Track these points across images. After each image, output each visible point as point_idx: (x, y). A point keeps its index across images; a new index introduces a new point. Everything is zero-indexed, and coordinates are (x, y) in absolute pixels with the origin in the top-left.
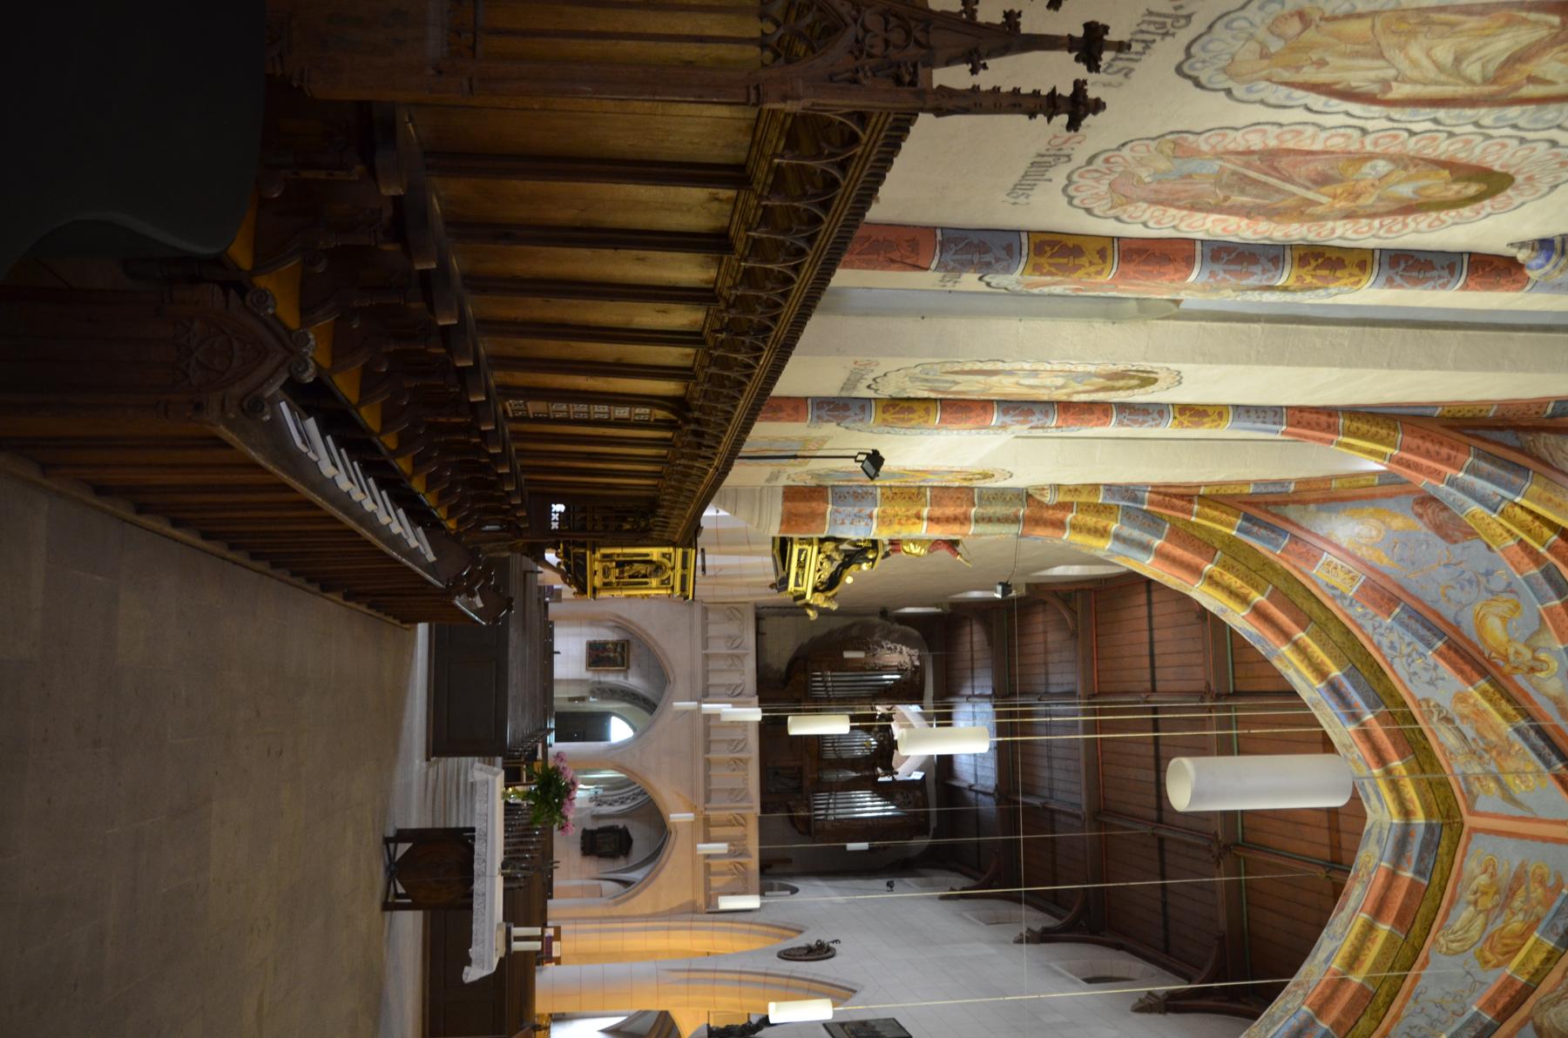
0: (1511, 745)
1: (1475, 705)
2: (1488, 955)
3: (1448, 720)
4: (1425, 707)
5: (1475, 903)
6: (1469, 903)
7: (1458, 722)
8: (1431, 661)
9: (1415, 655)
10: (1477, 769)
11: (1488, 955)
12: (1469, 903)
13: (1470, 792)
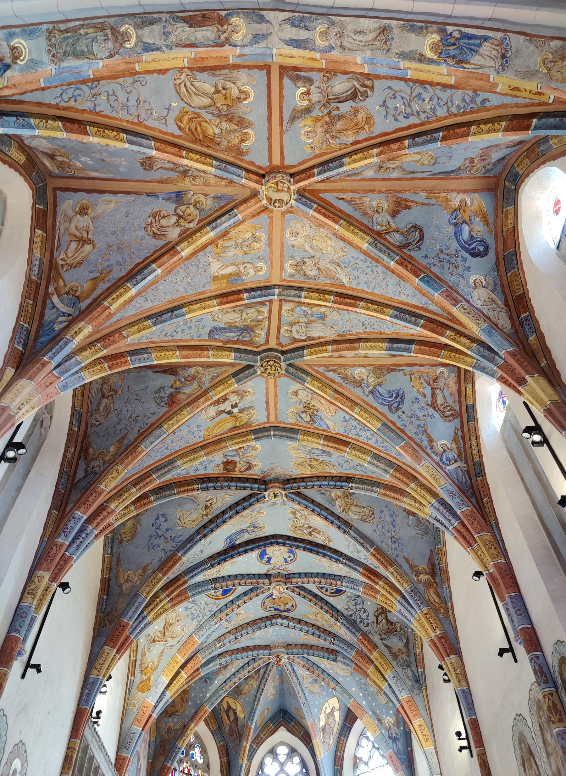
0: (333, 137)
1: (362, 128)
2: (186, 119)
3: (354, 96)
4: (368, 83)
5: (217, 92)
6: (216, 86)
7: (350, 103)
8: (400, 118)
9: (408, 110)
10: (315, 97)
11: (186, 119)
12: (216, 86)
13: (298, 78)
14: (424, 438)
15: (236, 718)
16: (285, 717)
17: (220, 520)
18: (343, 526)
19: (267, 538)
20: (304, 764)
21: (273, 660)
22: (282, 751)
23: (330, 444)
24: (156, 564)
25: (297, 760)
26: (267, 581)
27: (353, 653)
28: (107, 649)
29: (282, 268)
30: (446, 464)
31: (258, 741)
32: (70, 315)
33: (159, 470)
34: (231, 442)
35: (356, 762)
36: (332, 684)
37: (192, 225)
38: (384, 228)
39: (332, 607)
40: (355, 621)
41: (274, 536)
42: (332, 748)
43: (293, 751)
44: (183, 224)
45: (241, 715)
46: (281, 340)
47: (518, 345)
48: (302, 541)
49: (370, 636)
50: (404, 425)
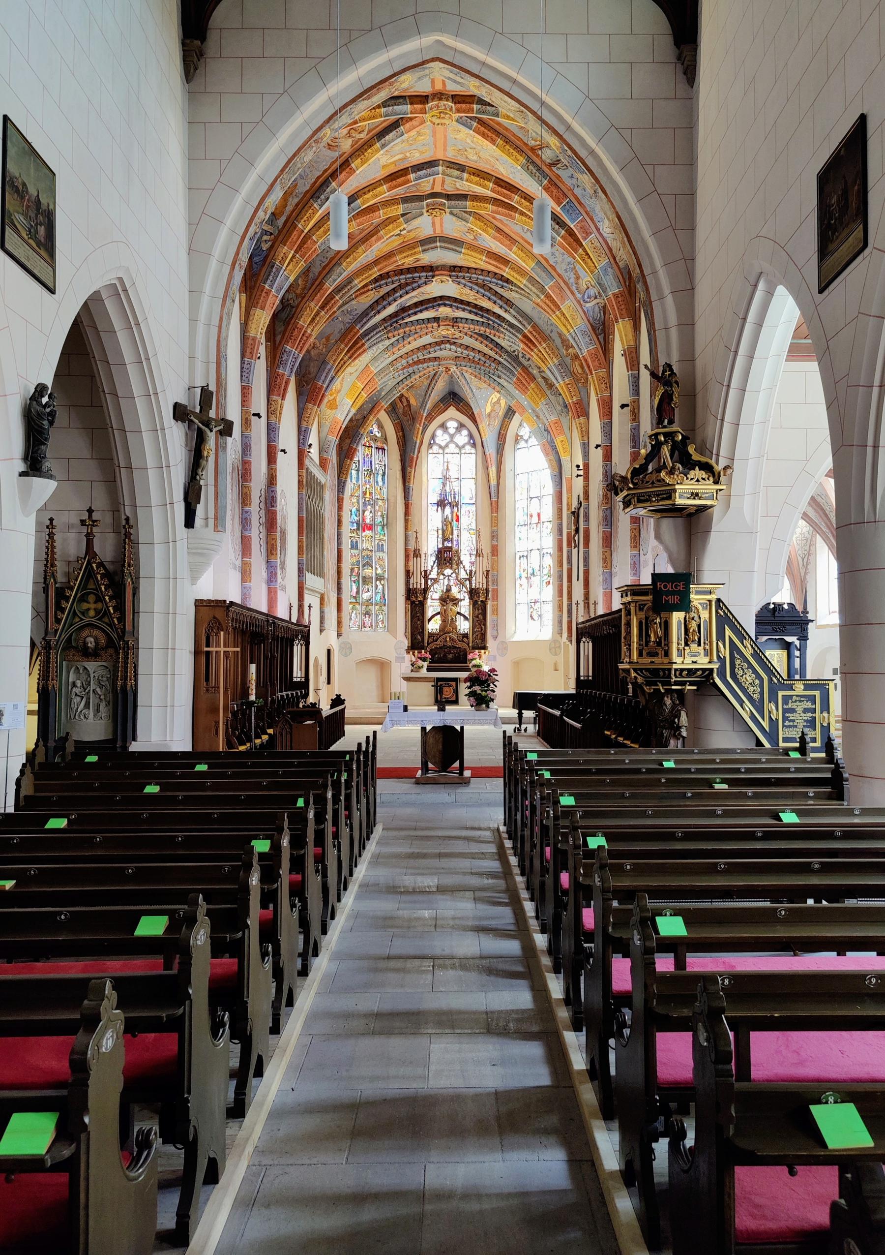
14: (573, 276)
15: (409, 405)
16: (454, 398)
17: (391, 298)
18: (505, 306)
19: (435, 299)
20: (471, 436)
21: (441, 369)
22: (452, 425)
23: (491, 262)
24: (338, 336)
25: (465, 432)
26: (435, 325)
27: (515, 379)
28: (310, 406)
29: (445, 150)
30: (587, 302)
31: (430, 418)
32: (271, 234)
33: (340, 291)
34: (400, 256)
35: (517, 439)
36: (497, 388)
37: (362, 136)
38: (538, 143)
39: (497, 345)
40: (517, 356)
41: (441, 298)
42: (497, 428)
43: (461, 426)
44: (354, 135)
45: (413, 402)
46: (445, 187)
47: (625, 282)
48: (468, 304)
49: (530, 369)
50: (556, 262)
